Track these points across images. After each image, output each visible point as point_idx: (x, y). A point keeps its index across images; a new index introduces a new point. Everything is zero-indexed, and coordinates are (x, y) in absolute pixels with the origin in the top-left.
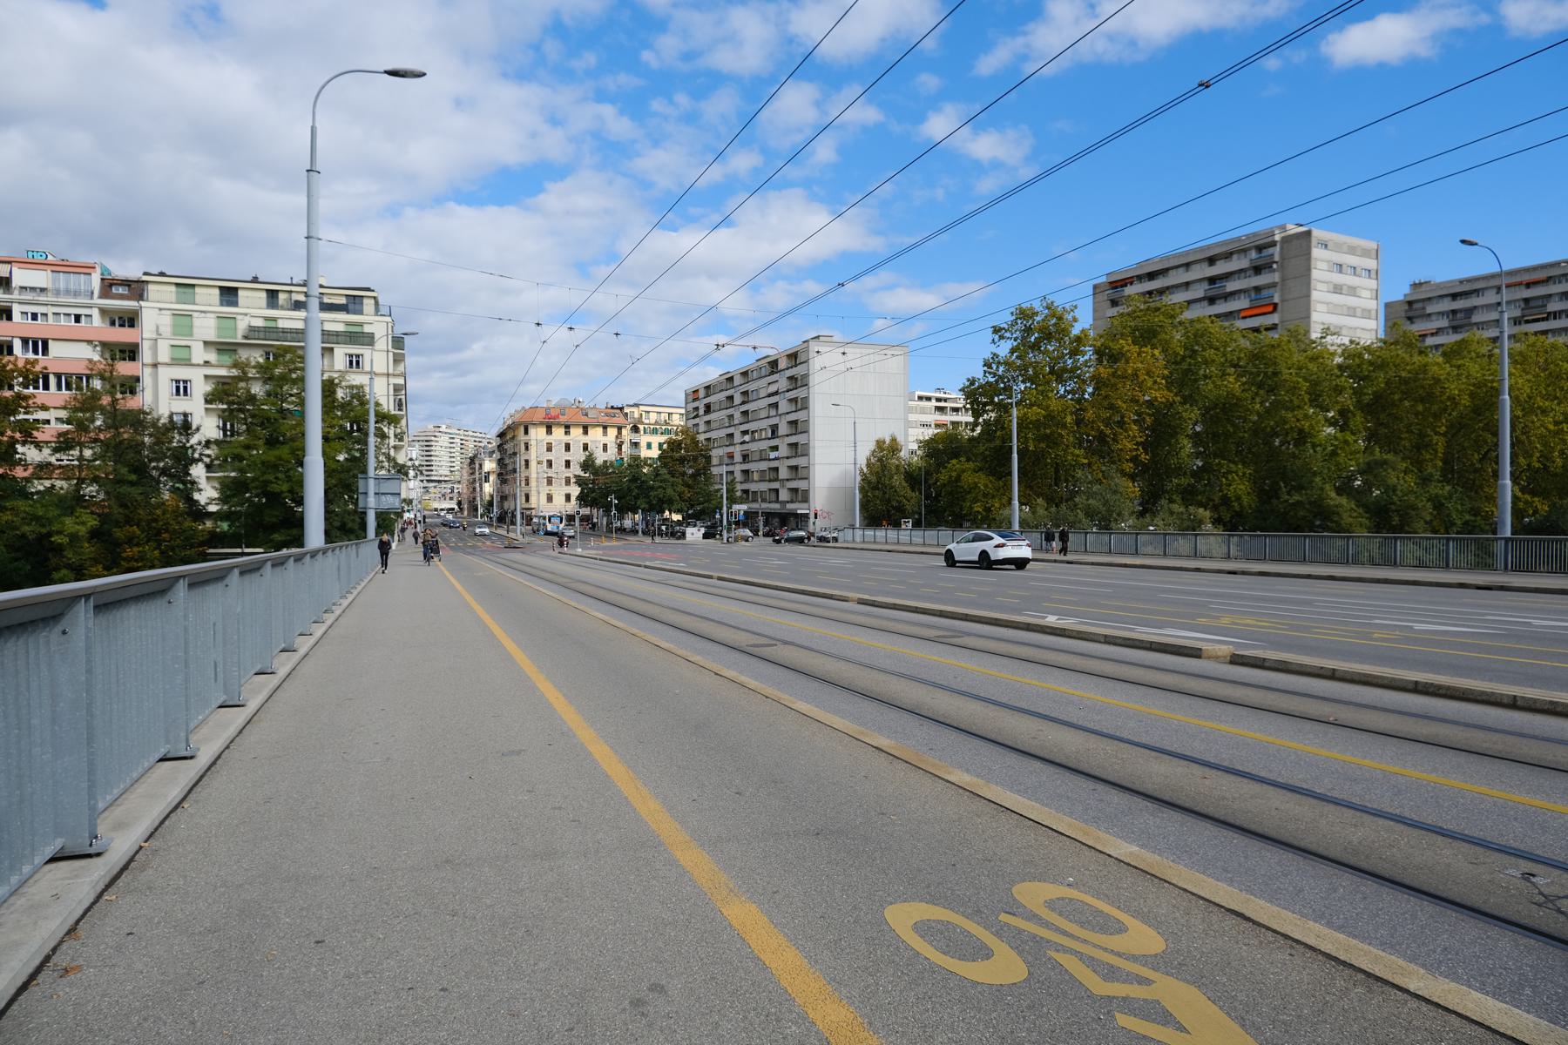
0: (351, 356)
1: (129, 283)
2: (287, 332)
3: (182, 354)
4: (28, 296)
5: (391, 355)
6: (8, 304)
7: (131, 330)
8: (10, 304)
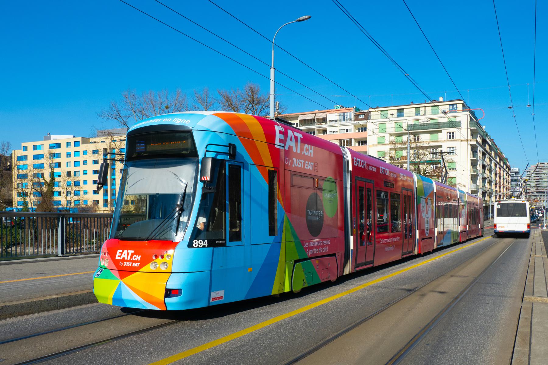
0: (450, 133)
3: (381, 140)
4: (332, 123)
5: (469, 130)
6: (325, 128)
8: (326, 128)
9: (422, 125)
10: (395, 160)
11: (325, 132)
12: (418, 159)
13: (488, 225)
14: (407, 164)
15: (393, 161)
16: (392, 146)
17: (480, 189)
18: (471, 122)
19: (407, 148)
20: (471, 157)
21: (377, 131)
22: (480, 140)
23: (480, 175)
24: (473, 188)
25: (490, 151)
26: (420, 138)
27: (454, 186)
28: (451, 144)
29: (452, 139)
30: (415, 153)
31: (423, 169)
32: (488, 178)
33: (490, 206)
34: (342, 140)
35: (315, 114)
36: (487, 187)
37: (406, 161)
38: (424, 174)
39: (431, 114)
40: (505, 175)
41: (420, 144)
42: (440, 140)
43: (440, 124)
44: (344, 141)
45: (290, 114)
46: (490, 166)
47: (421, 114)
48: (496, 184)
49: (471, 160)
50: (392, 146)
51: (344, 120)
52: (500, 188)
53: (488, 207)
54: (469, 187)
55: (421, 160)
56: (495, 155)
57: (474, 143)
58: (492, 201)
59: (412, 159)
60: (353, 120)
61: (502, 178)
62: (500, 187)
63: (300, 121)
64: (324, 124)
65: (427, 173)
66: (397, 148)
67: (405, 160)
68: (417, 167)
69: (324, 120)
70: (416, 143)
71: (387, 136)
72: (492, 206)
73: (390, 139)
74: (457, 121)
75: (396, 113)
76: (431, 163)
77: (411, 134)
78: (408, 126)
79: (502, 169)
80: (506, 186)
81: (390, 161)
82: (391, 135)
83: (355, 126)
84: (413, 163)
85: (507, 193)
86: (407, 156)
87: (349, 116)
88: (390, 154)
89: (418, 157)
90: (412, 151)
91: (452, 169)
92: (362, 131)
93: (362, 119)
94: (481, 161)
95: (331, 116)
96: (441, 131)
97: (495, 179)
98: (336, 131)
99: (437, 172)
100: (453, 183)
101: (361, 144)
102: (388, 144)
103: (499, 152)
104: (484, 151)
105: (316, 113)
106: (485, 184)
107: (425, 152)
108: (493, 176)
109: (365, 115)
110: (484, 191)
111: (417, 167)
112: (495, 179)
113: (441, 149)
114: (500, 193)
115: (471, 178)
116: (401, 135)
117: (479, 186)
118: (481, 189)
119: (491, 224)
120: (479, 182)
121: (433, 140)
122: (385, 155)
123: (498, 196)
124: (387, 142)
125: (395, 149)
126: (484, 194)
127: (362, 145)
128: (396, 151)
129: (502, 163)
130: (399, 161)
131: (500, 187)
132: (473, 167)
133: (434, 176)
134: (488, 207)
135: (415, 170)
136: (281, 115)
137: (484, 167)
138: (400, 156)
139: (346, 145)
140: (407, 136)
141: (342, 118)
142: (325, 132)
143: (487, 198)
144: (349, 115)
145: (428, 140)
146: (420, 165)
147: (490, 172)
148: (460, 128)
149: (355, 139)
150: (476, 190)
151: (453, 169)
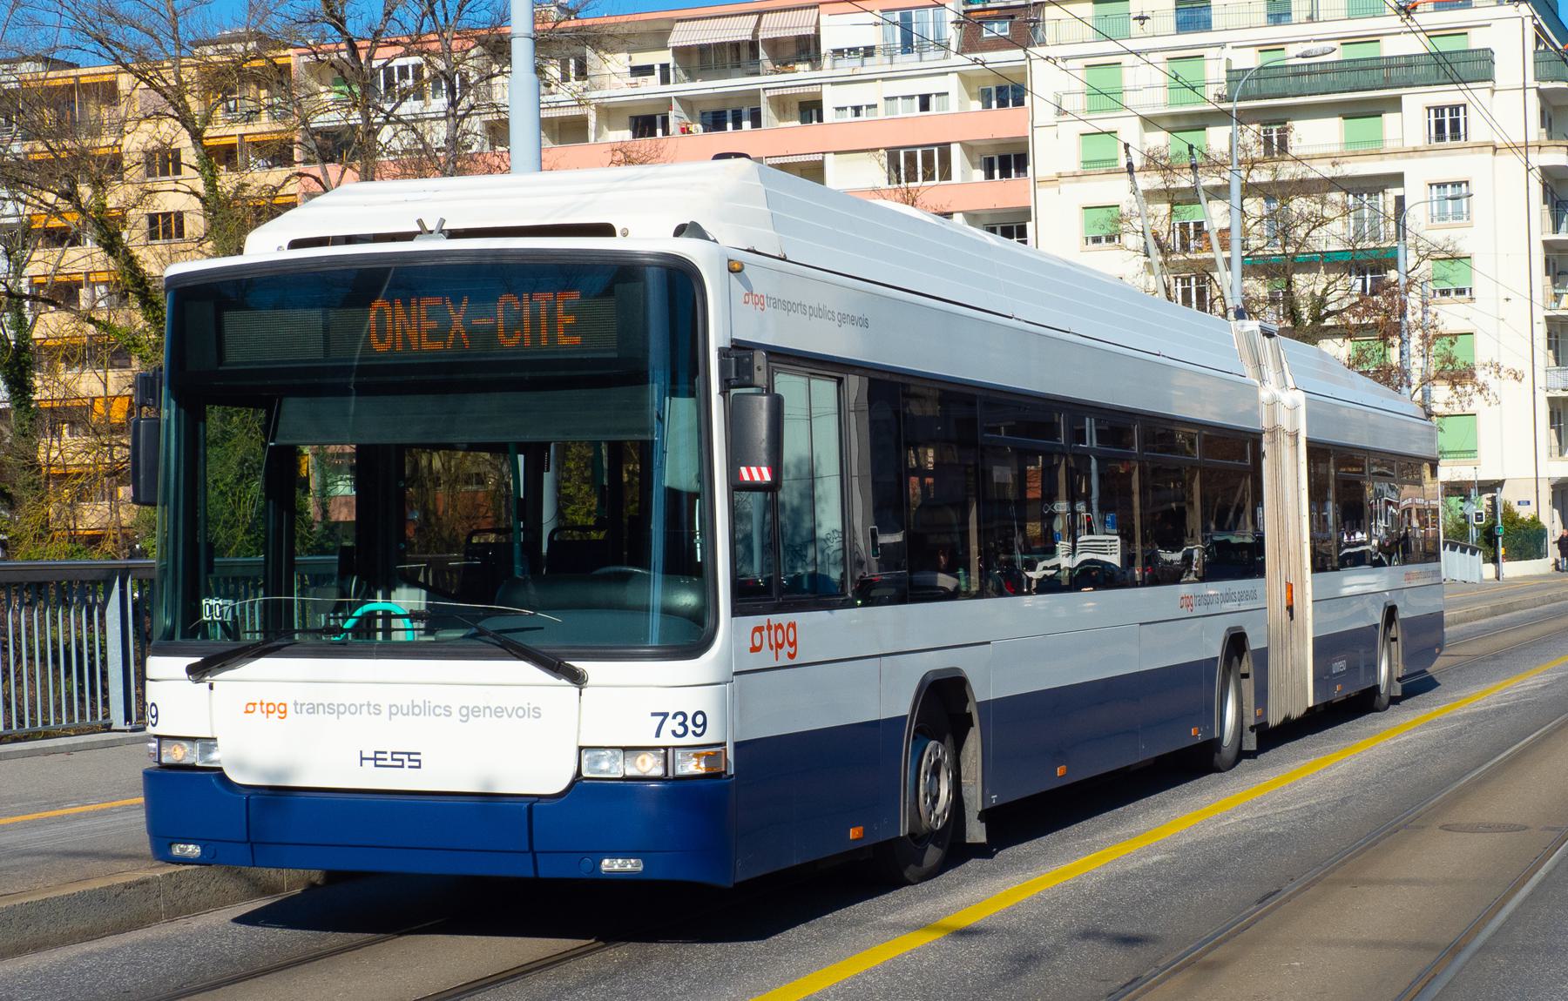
0: (1439, 110)
1: (1010, 12)
2: (1303, 74)
3: (1101, 149)
4: (846, 66)
5: (1533, 97)
6: (811, 89)
8: (815, 89)
10: (1173, 252)
11: (814, 112)
12: (1286, 244)
16: (1155, 181)
19: (1227, 188)
21: (1075, 103)
28: (1449, 164)
29: (1452, 139)
30: (1272, 215)
31: (1313, 293)
34: (902, 153)
35: (756, 17)
38: (1317, 318)
39: (1343, 14)
41: (1293, 170)
42: (1390, 146)
43: (1390, 63)
44: (911, 159)
45: (624, 19)
47: (1295, 17)
49: (1547, 244)
50: (1155, 181)
51: (907, 46)
55: (1304, 249)
59: (1254, 243)
60: (954, 47)
63: (682, 53)
64: (803, 71)
65: (1329, 314)
66: (1178, 190)
68: (1280, 283)
69: (806, 49)
70: (1274, 164)
71: (1130, 129)
74: (1473, 51)
75: (1173, 12)
76: (1347, 263)
77: (1245, 117)
78: (1234, 75)
82: (1149, 122)
83: (964, 78)
84: (1260, 263)
86: (1228, 230)
87: (931, 26)
89: (1285, 232)
90: (1255, 206)
91: (1453, 293)
92: (1003, 103)
93: (999, 44)
95: (838, 30)
96: (1395, 104)
98: (868, 107)
99: (1376, 304)
100: (1460, 365)
101: (997, 172)
105: (760, 13)
107: (1319, 207)
109: (1017, 19)
111: (1280, 283)
113: (1398, 191)
115: (1549, 335)
116: (1200, 121)
121: (1360, 149)
122: (1121, 226)
125: (1177, 198)
127: (1005, 173)
128: (1173, 204)
132: (1554, 282)
133: (1363, 329)
135: (1273, 301)
136: (579, 23)
139: (920, 177)
140: (1227, 130)
141: (898, 39)
142: (814, 112)
144: (931, 19)
145: (1336, 149)
146: (1295, 276)
148: (1489, 84)
149: (968, 148)
151: (1460, 292)
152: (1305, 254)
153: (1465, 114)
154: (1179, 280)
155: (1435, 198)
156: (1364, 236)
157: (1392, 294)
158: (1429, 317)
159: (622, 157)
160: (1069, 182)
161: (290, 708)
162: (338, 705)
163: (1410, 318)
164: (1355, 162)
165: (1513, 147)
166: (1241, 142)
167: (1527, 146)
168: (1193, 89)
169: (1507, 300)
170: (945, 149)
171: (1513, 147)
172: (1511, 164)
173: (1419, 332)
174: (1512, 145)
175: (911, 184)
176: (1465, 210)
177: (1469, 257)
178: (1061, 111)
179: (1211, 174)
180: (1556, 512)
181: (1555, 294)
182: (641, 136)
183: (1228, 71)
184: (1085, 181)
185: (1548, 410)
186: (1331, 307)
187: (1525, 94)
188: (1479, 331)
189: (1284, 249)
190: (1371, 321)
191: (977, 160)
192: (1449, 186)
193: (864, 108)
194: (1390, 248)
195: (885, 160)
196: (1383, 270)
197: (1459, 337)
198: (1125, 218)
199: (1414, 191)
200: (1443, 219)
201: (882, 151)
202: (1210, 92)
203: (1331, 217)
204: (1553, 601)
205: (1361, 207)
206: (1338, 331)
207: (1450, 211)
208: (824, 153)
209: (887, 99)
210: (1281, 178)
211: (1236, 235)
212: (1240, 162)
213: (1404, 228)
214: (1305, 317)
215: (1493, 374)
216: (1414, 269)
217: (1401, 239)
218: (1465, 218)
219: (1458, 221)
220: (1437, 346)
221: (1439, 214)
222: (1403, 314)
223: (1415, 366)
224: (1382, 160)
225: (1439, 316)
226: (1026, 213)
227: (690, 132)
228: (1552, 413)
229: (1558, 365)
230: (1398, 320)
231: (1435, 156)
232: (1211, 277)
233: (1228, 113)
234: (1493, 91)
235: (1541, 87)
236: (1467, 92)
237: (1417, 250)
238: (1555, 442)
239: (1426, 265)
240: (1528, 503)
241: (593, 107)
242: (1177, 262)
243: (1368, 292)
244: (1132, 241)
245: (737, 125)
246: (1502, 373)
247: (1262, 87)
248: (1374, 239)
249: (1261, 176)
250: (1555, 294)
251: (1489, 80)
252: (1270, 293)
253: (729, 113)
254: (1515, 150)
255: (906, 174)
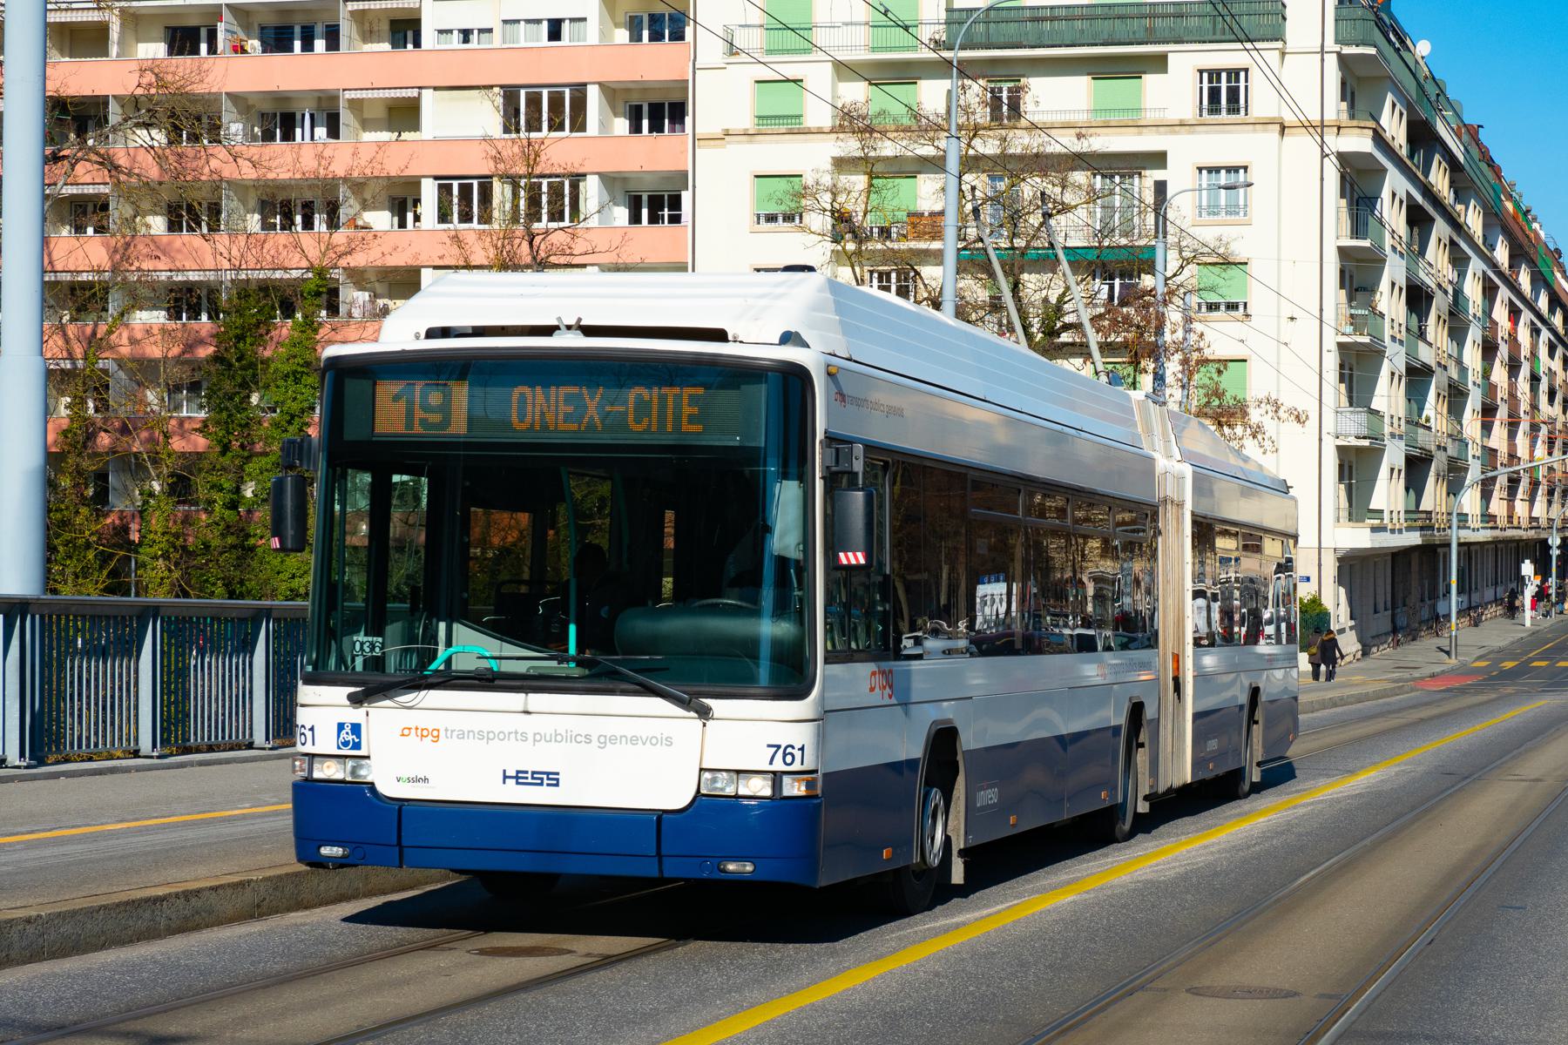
0: (1214, 74)
2: (1044, 19)
3: (781, 101)
5: (1332, 62)
7: (677, 45)
9: (1041, 13)
10: (869, 238)
11: (410, 34)
12: (1014, 235)
13: (1437, 669)
14: (941, 263)
15: (851, 246)
16: (850, 146)
17: (1393, 435)
18: (1345, 12)
20: (1338, 233)
22: (1395, 128)
23: (1391, 348)
24: (1352, 428)
25: (1458, 199)
26: (1027, 104)
27: (1233, 415)
31: (1046, 300)
32: (1439, 370)
33: (1449, 545)
34: (523, 92)
36: (1432, 423)
37: (936, 245)
38: (1051, 333)
40: (1543, 351)
41: (1026, 141)
42: (1150, 117)
44: (534, 101)
46: (1458, 293)
48: (1488, 411)
49: (1343, 251)
50: (850, 146)
52: (1512, 435)
53: (1439, 550)
54: (1329, 425)
55: (1036, 243)
56: (1486, 226)
57: (1361, 143)
58: (1463, 518)
61: (1525, 372)
62: (1513, 426)
65: (1066, 327)
66: (878, 159)
67: (933, 239)
70: (1003, 132)
71: (818, 76)
72: (1460, 545)
73: (835, 96)
76: (1090, 263)
77: (966, 70)
78: (956, 15)
79: (1526, 316)
80: (1551, 422)
81: (835, 241)
82: (845, 70)
85: (1551, 469)
86: (942, 213)
88: (834, 195)
91: (1223, 308)
92: (656, 37)
94: (1404, 263)
96: (1159, 63)
97: (1486, 374)
98: (481, 31)
99: (1127, 319)
100: (1228, 400)
101: (645, 123)
102: (820, 132)
103: (1509, 206)
104: (1419, 198)
106: (1421, 409)
107: (1058, 190)
108: (1472, 356)
110: (1416, 453)
112: (1486, 374)
113: (1158, 175)
114: (1511, 465)
115: (1342, 366)
116: (905, 73)
117: (1387, 420)
118: (1401, 437)
119: (1453, 661)
120: (1388, 396)
121: (1114, 118)
122: (804, 202)
123: (1497, 486)
124: (819, 115)
125: (875, 169)
126: (1416, 468)
127: (656, 127)
129: (1524, 280)
130: (895, 246)
131: (1513, 426)
132: (1351, 299)
134: (1439, 550)
137: (1417, 298)
138: (902, 216)
139: (545, 125)
140: (946, 84)
142: (410, 34)
143: (1433, 496)
145: (1081, 118)
146: (1025, 276)
147: (1457, 332)
148: (1279, 44)
149: (611, 92)
150: (1366, 443)
151: (1232, 307)
152: (1038, 249)
153: (1246, 81)
154: (876, 275)
155: (1204, 186)
156: (1113, 230)
157: (1147, 306)
158: (1193, 338)
159: (153, 80)
160: (739, 142)
161: (442, 734)
162: (488, 733)
163: (1168, 337)
164: (1107, 135)
165: (1307, 126)
166: (962, 103)
167: (1323, 126)
168: (906, 28)
169: (1292, 319)
170: (579, 92)
171: (1307, 126)
172: (1303, 147)
173: (1178, 357)
174: (1307, 124)
175: (533, 135)
176: (1241, 202)
177: (1246, 263)
178: (732, 50)
179: (922, 141)
180: (1342, 591)
181: (1352, 316)
182: (180, 53)
183: (948, 10)
184: (760, 142)
185: (1337, 462)
186: (1069, 319)
187: (1323, 60)
188: (1254, 357)
189: (1012, 242)
190: (1119, 340)
191: (621, 107)
192: (1223, 172)
193: (476, 32)
194: (1145, 247)
195: (500, 101)
196: (1135, 273)
197: (1230, 364)
198: (808, 191)
199: (1178, 176)
200: (1215, 214)
201: (496, 90)
202: (926, 33)
203: (1073, 203)
204: (1335, 705)
205: (1112, 193)
206: (1077, 350)
207: (1223, 202)
208: (420, 88)
209: (505, 22)
210: (1011, 151)
211: (951, 221)
212: (960, 128)
213: (1165, 218)
214: (1034, 330)
215: (1270, 414)
216: (1175, 275)
217: (1161, 236)
218: (1242, 213)
219: (1233, 217)
220: (1201, 375)
221: (1209, 206)
222: (1159, 330)
223: (1172, 399)
224: (1140, 134)
225: (1205, 337)
226: (681, 179)
227: (244, 51)
228: (1341, 467)
229: (1351, 405)
230: (1153, 339)
231: (1207, 132)
232: (917, 273)
233: (949, 62)
234: (1283, 54)
235: (1344, 52)
236: (1254, 53)
237: (1181, 252)
238: (1344, 503)
239: (1191, 269)
240: (1308, 579)
241: (116, 12)
242: (873, 251)
243: (1116, 302)
244: (819, 222)
245: (308, 46)
246: (1281, 413)
247: (991, 31)
248: (1125, 234)
249: (987, 146)
250: (1352, 316)
251: (1277, 40)
252: (991, 297)
253: (297, 30)
254: (1311, 130)
255: (528, 122)
